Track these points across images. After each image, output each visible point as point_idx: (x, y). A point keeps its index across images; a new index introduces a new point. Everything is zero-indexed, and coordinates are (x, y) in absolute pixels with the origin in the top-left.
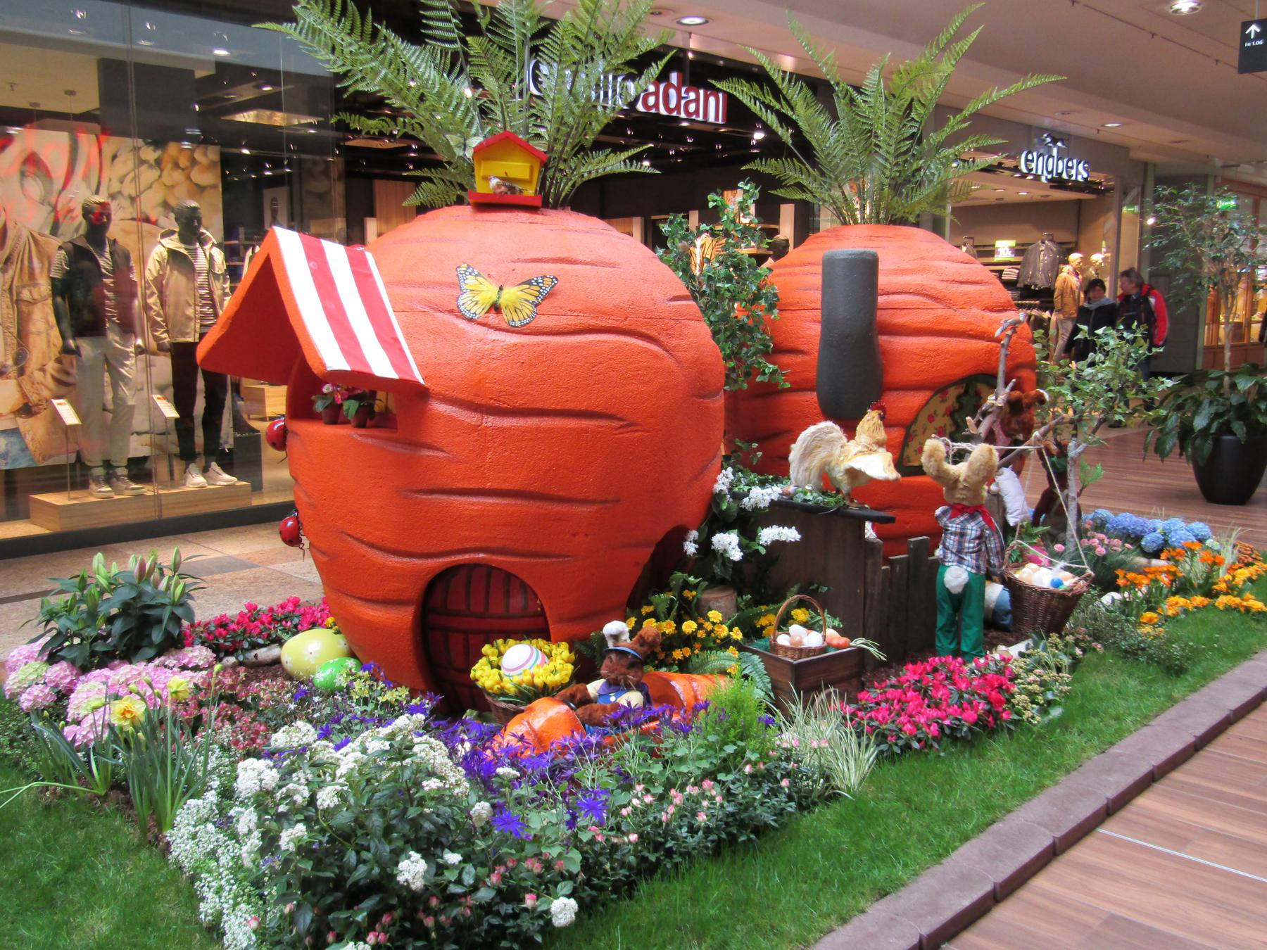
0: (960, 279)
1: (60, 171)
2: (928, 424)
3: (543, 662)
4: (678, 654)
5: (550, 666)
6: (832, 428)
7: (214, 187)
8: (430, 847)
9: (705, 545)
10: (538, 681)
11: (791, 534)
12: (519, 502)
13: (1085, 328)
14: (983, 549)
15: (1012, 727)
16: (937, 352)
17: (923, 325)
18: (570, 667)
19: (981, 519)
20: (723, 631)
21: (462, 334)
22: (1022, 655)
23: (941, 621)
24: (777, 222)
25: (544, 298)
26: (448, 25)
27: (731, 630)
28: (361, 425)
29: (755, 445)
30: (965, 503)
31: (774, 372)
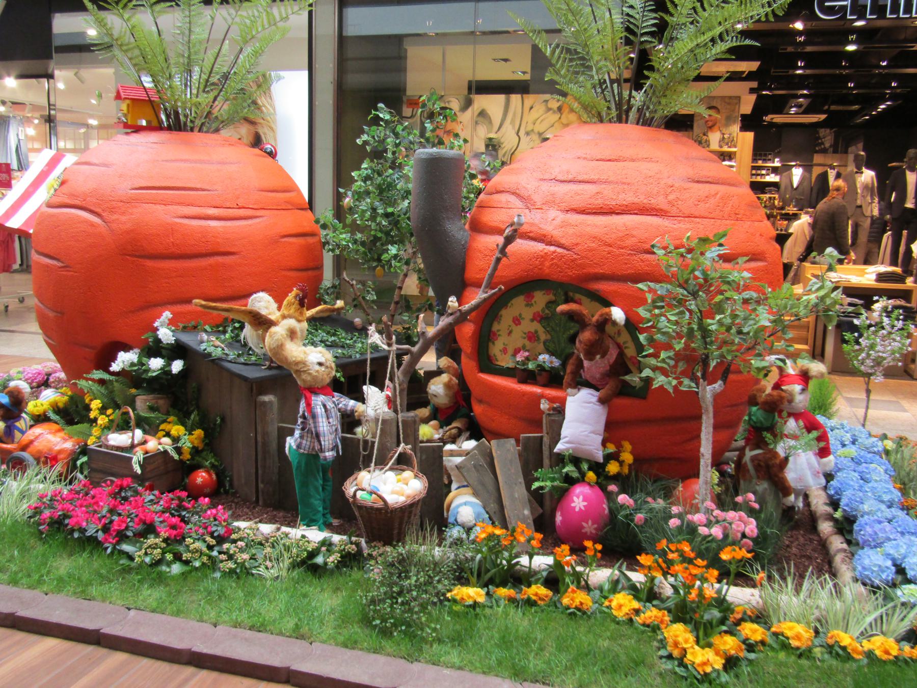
1: (496, 120)
2: (514, 327)
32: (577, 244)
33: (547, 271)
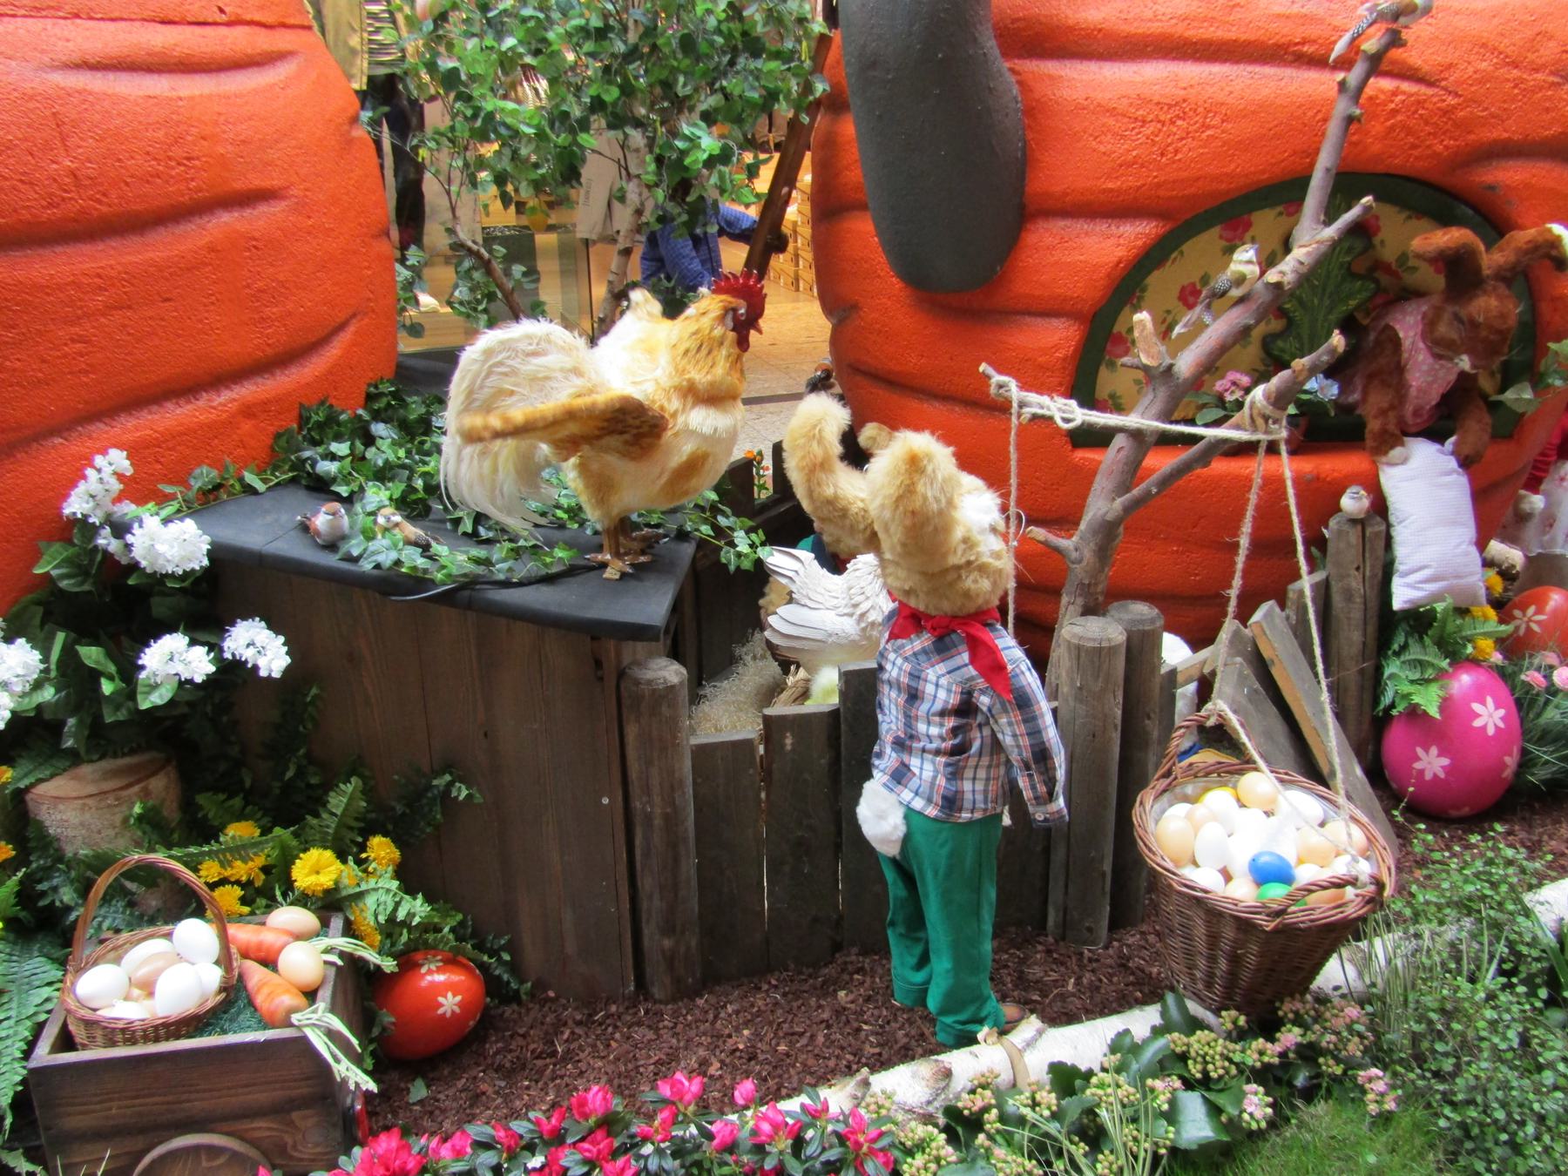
6: (547, 339)
16: (1178, 108)
17: (1155, 28)
19: (965, 657)
32: (1450, 66)
33: (1376, 148)
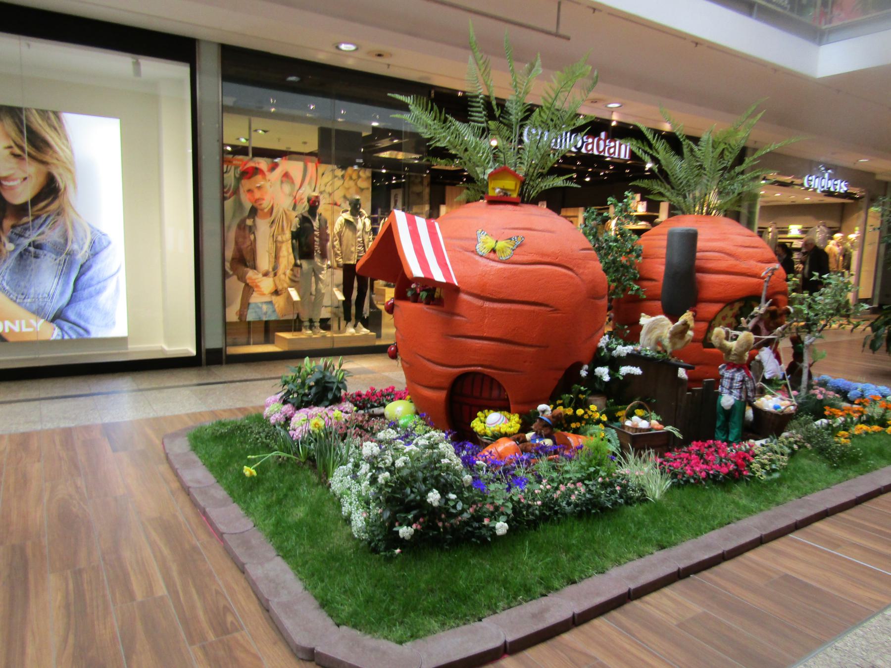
0: (746, 245)
3: (506, 423)
4: (573, 425)
5: (509, 424)
7: (368, 189)
8: (444, 490)
9: (591, 372)
10: (503, 431)
11: (637, 371)
12: (499, 344)
13: (817, 274)
14: (744, 387)
15: (749, 479)
16: (728, 283)
17: (722, 269)
18: (518, 426)
20: (597, 416)
21: (477, 262)
22: (762, 445)
23: (718, 424)
24: (658, 212)
25: (517, 247)
26: (480, 115)
27: (601, 415)
28: (428, 303)
29: (626, 327)
30: (735, 362)
31: (638, 290)
